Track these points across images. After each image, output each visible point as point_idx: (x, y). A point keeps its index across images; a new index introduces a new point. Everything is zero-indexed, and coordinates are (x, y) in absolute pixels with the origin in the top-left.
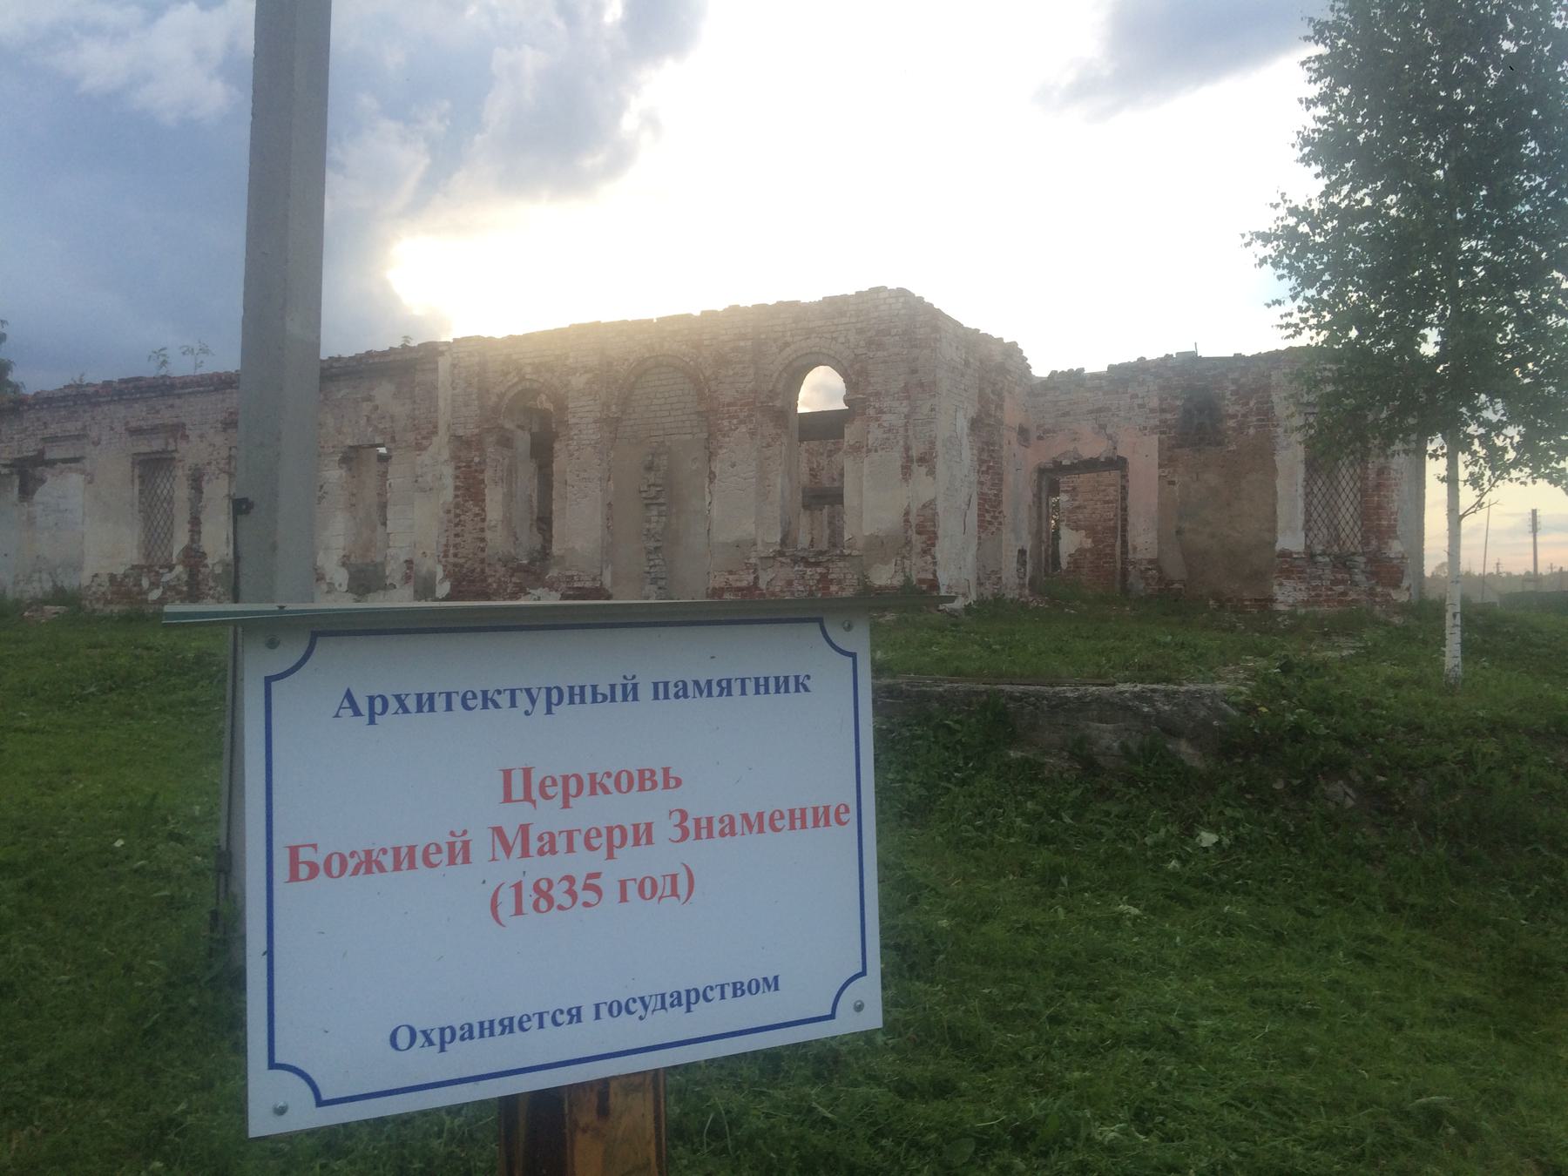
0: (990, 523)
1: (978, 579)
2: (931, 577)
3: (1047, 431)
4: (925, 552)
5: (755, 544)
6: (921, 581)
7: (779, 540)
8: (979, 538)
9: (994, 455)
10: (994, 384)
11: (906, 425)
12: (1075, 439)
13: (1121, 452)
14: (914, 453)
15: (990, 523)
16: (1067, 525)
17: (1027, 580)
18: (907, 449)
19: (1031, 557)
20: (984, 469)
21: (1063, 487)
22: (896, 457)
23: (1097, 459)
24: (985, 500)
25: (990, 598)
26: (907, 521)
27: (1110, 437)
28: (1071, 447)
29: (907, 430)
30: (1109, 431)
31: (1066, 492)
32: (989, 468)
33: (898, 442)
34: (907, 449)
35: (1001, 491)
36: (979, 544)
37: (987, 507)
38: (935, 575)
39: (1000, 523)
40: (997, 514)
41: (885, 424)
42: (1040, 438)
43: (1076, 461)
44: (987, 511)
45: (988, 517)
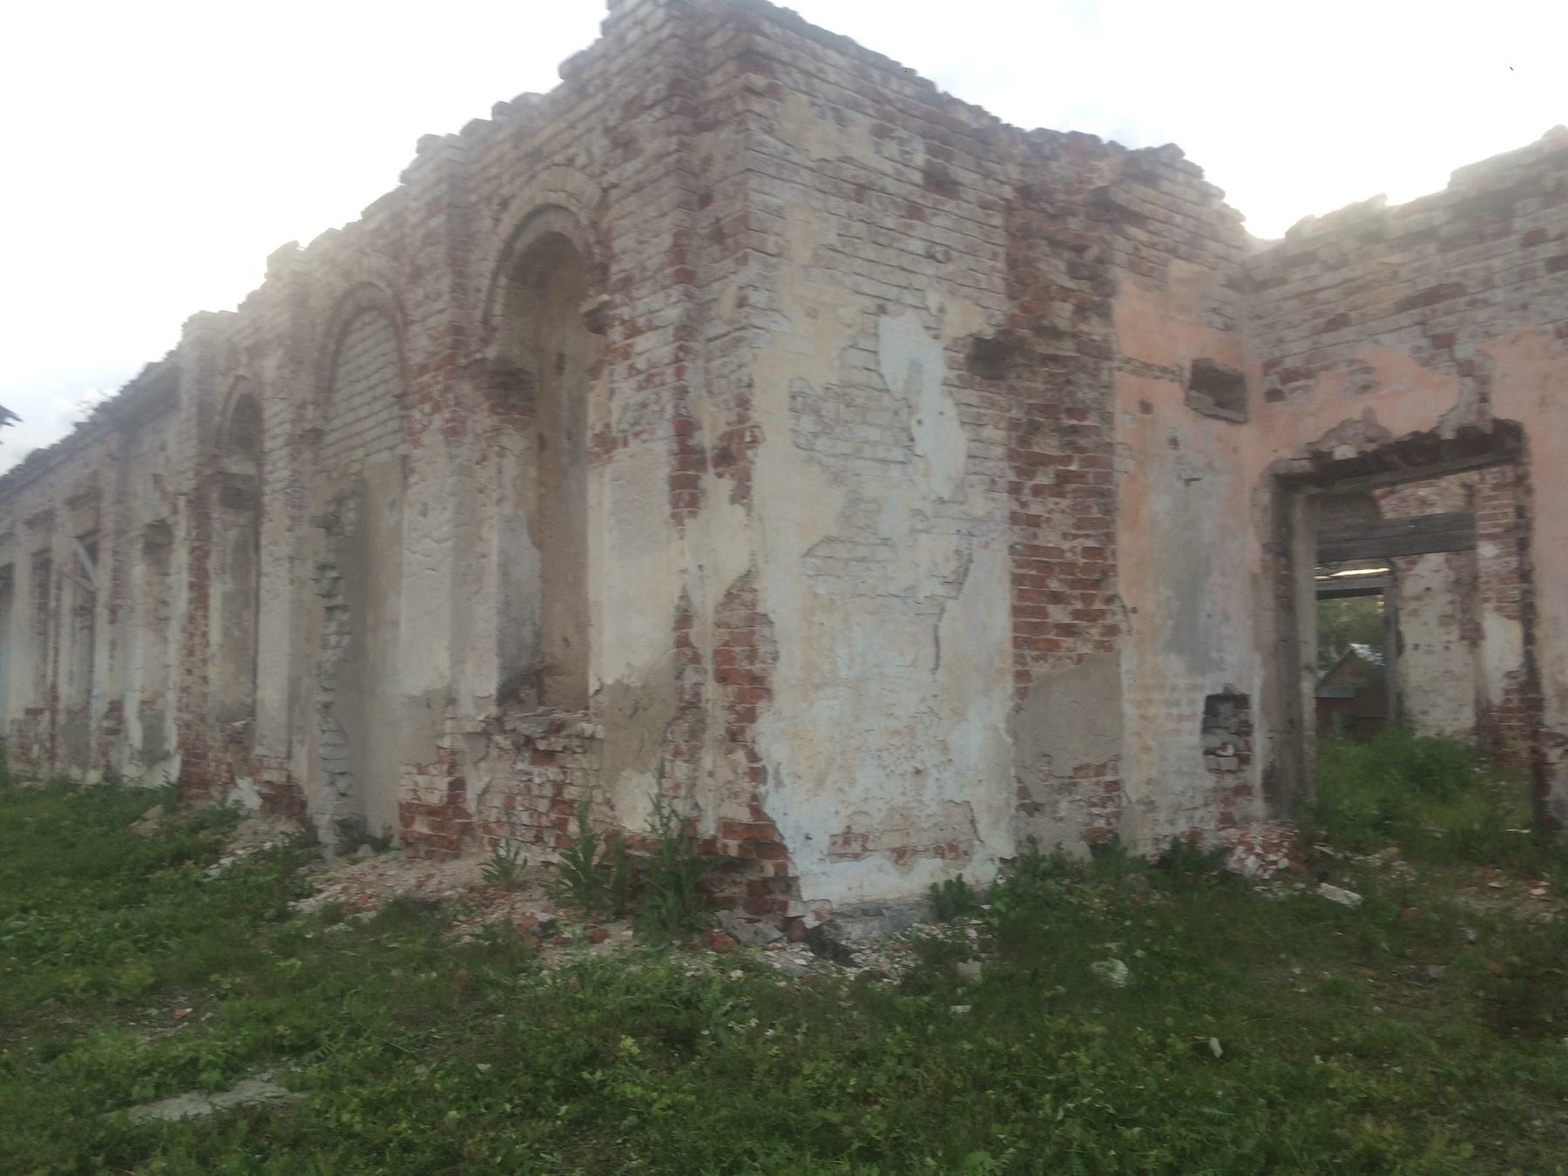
0: (1068, 630)
1: (1023, 792)
2: (745, 816)
3: (1289, 376)
4: (734, 736)
5: (452, 701)
6: (728, 827)
7: (493, 691)
8: (1022, 676)
9: (1083, 442)
10: (1080, 250)
11: (678, 360)
12: (1366, 388)
13: (1504, 408)
14: (707, 439)
15: (1068, 630)
16: (1499, 609)
17: (1255, 774)
18: (685, 428)
19: (1265, 709)
20: (1044, 478)
21: (1484, 527)
22: (659, 449)
23: (1433, 435)
24: (1047, 568)
25: (1080, 851)
26: (683, 642)
27: (1466, 369)
28: (1354, 409)
29: (679, 373)
30: (1463, 351)
31: (1491, 537)
32: (1063, 478)
33: (662, 410)
34: (685, 428)
35: (1110, 538)
36: (1022, 693)
37: (1054, 585)
38: (756, 811)
39: (1112, 630)
40: (1098, 605)
41: (641, 364)
42: (1274, 395)
43: (1371, 447)
44: (1056, 598)
45: (1058, 614)
